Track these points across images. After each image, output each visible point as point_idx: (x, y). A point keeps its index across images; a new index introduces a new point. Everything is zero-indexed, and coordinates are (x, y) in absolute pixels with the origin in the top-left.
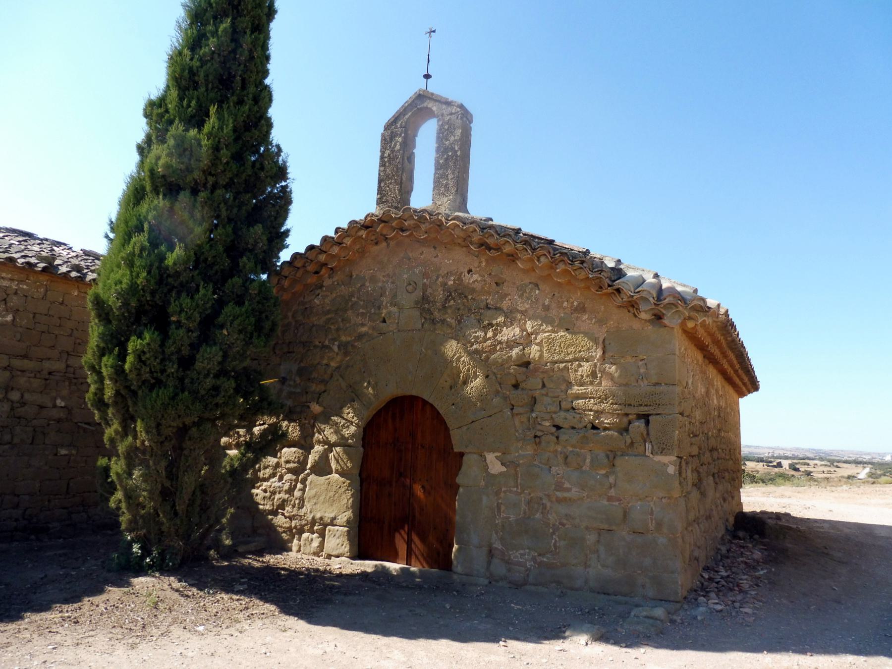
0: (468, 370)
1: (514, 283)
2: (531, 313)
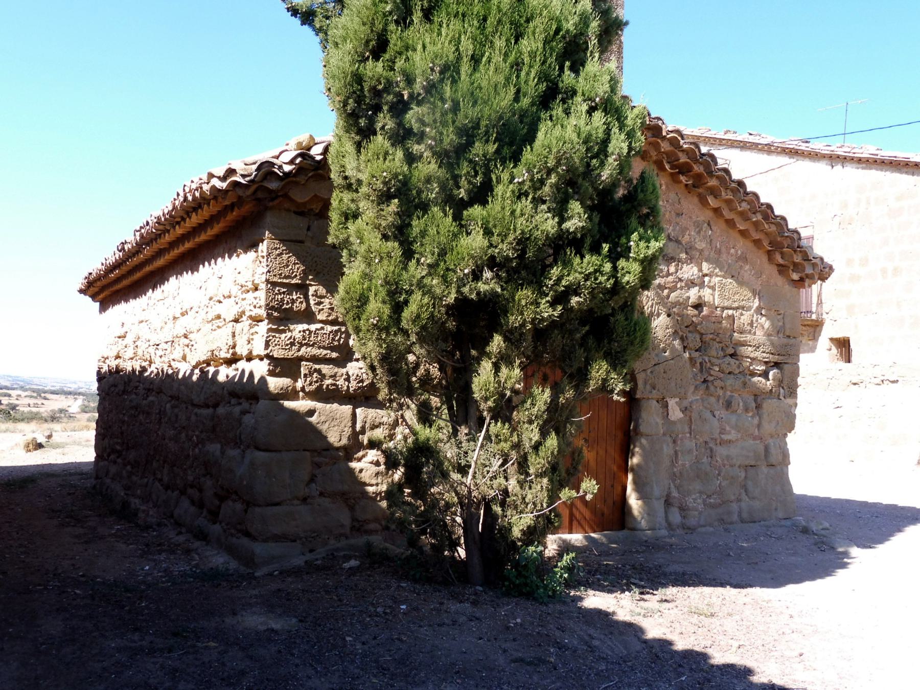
0: (652, 306)
1: (691, 218)
2: (706, 253)
